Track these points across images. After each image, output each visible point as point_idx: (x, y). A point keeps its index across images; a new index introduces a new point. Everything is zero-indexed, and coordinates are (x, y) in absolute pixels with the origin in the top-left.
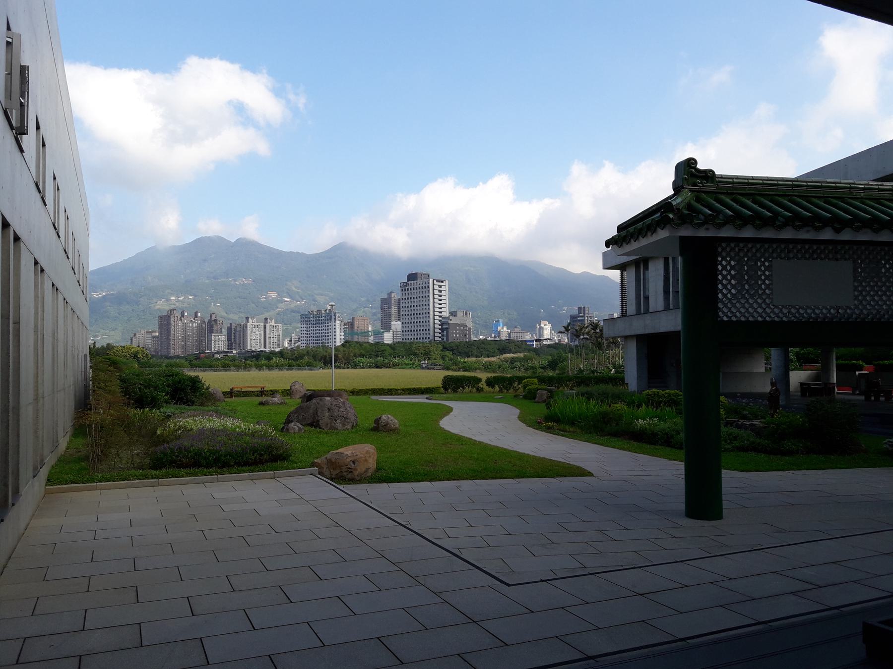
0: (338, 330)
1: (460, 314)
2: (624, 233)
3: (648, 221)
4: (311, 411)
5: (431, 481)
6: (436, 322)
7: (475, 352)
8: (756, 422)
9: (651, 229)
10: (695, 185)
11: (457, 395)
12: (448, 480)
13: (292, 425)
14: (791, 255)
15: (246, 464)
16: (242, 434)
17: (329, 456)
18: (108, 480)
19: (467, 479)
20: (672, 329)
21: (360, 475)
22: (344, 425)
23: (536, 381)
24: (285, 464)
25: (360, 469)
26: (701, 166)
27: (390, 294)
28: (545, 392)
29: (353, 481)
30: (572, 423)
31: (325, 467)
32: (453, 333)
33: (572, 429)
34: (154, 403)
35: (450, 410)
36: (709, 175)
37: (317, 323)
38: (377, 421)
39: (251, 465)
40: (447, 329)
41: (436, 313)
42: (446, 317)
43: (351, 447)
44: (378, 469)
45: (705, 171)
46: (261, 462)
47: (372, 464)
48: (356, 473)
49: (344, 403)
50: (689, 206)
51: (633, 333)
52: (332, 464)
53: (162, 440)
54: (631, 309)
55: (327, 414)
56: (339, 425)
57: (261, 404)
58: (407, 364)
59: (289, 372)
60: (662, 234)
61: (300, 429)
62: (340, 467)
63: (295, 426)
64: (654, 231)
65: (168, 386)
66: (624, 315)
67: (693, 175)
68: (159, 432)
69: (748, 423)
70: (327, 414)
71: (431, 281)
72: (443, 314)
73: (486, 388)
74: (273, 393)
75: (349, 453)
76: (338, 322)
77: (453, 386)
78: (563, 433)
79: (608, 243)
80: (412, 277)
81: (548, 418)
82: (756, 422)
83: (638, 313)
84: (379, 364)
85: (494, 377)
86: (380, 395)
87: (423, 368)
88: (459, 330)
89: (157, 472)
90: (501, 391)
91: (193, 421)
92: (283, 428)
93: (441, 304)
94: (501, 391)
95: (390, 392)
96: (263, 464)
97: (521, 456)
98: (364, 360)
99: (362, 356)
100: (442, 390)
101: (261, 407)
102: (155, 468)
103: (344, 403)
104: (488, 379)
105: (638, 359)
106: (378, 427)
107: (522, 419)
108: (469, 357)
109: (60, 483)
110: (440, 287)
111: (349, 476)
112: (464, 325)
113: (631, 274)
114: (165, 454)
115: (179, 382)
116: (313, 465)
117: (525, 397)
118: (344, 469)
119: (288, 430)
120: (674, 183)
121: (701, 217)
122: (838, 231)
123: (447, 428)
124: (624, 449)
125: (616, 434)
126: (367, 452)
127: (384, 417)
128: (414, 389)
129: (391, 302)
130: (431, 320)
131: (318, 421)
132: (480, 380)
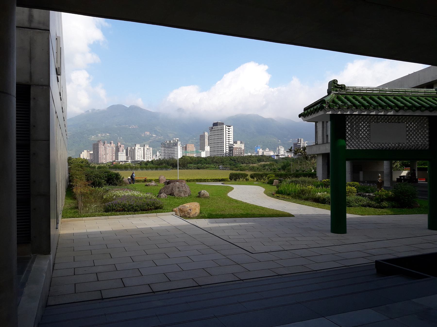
1: (239, 142)
2: (306, 112)
3: (315, 107)
4: (170, 188)
5: (223, 218)
6: (227, 146)
7: (246, 161)
8: (371, 194)
9: (316, 111)
10: (336, 91)
11: (236, 182)
12: (231, 218)
13: (162, 194)
14: (379, 121)
15: (144, 210)
16: (141, 198)
17: (179, 207)
18: (87, 217)
19: (239, 217)
20: (327, 152)
21: (193, 215)
22: (185, 195)
23: (274, 175)
24: (161, 210)
25: (193, 213)
26: (339, 83)
28: (277, 181)
29: (190, 218)
30: (289, 195)
31: (178, 212)
33: (288, 197)
34: (100, 185)
35: (232, 189)
36: (343, 87)
38: (199, 193)
39: (146, 210)
40: (232, 150)
41: (227, 142)
43: (189, 204)
44: (201, 213)
45: (341, 85)
46: (151, 209)
47: (198, 211)
48: (191, 215)
49: (184, 185)
50: (333, 101)
51: (320, 153)
52: (181, 211)
53: (106, 201)
54: (320, 141)
55: (177, 190)
56: (182, 195)
57: (146, 185)
58: (212, 167)
59: (156, 171)
60: (321, 113)
61: (165, 196)
62: (184, 212)
63: (163, 195)
64: (318, 112)
65: (106, 177)
66: (316, 144)
67: (336, 87)
68: (104, 197)
69: (367, 194)
70: (177, 190)
71: (225, 126)
73: (250, 179)
74: (151, 181)
75: (188, 206)
76: (179, 147)
77: (234, 178)
78: (284, 199)
79: (300, 116)
80: (215, 124)
81: (278, 192)
82: (371, 194)
83: (323, 143)
84: (199, 167)
85: (254, 174)
86: (200, 182)
88: (238, 150)
89: (107, 213)
90: (257, 180)
91: (119, 193)
92: (158, 196)
94: (257, 180)
95: (205, 181)
96: (152, 210)
97: (263, 208)
98: (192, 165)
99: (191, 163)
100: (229, 180)
101: (146, 187)
102: (106, 212)
103: (184, 185)
104: (251, 174)
105: (323, 165)
106: (200, 196)
107: (265, 193)
108: (243, 164)
109: (67, 218)
110: (229, 129)
111: (188, 216)
112: (240, 148)
113: (320, 125)
114: (109, 206)
115: (110, 175)
116: (173, 211)
117: (268, 183)
118: (186, 213)
119: (160, 197)
120: (328, 90)
121: (338, 106)
122: (397, 111)
123: (230, 197)
124: (310, 206)
125: (307, 199)
126: (196, 206)
127: (202, 191)
128: (216, 179)
131: (173, 193)
132: (247, 175)
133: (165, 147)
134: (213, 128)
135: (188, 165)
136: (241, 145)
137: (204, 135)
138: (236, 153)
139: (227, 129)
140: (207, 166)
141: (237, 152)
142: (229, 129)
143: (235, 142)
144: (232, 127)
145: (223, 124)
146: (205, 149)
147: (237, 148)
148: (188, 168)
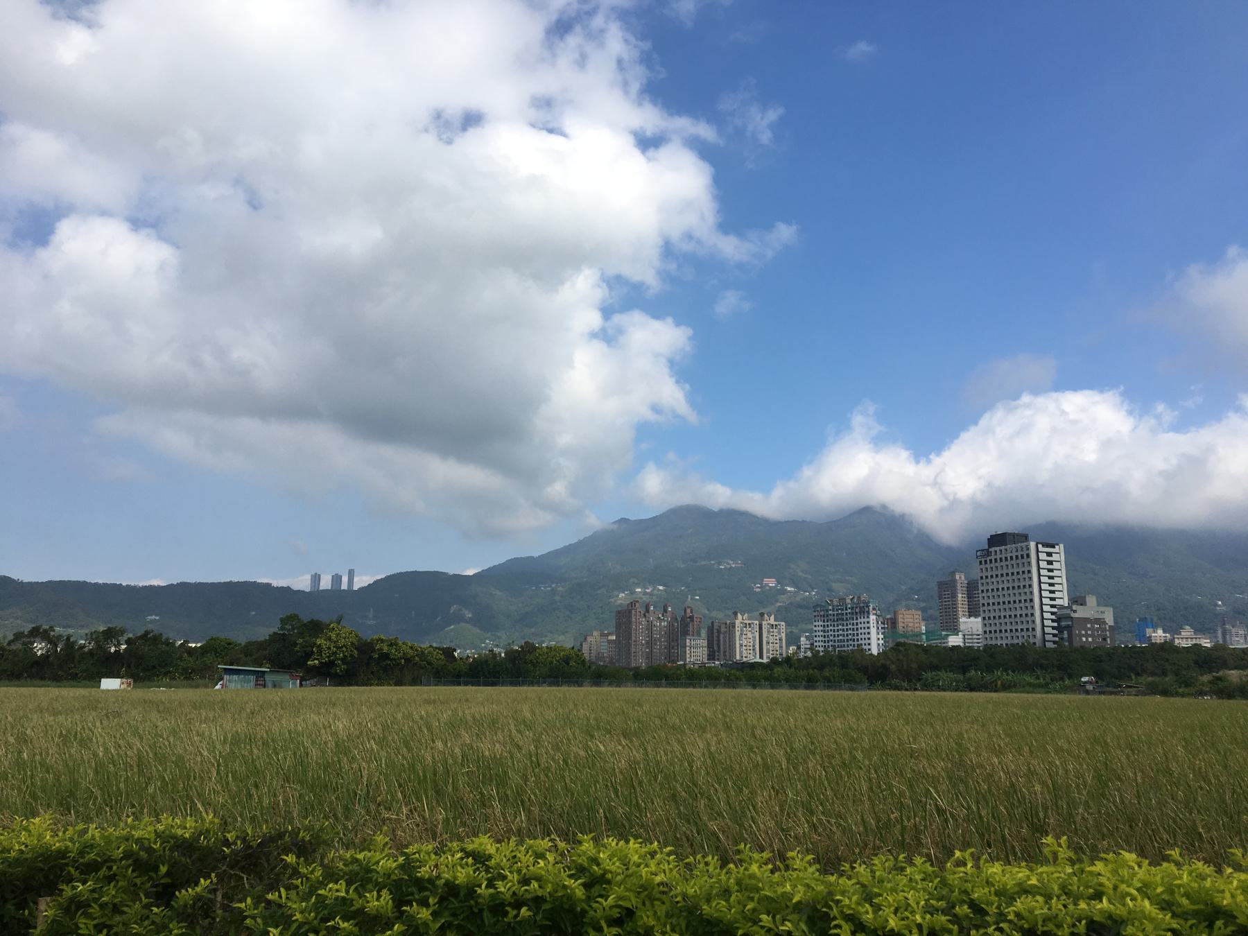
0: (873, 631)
1: (1091, 600)
27: (953, 574)
32: (1081, 636)
37: (840, 618)
41: (1045, 601)
42: (1062, 607)
58: (1030, 685)
71: (1032, 545)
72: (1058, 602)
76: (873, 618)
80: (997, 540)
87: (1087, 692)
88: (1092, 629)
93: (1052, 585)
98: (943, 674)
108: (1137, 674)
110: (1049, 554)
112: (1101, 621)
129: (955, 586)
130: (1037, 613)
133: (825, 617)
134: (989, 554)
135: (929, 675)
136: (1102, 609)
137: (954, 581)
138: (1086, 639)
139: (1043, 556)
140: (1009, 677)
141: (1087, 636)
142: (1049, 554)
143: (1077, 600)
144: (1060, 548)
145: (1024, 537)
146: (962, 627)
147: (1086, 620)
148: (927, 687)
